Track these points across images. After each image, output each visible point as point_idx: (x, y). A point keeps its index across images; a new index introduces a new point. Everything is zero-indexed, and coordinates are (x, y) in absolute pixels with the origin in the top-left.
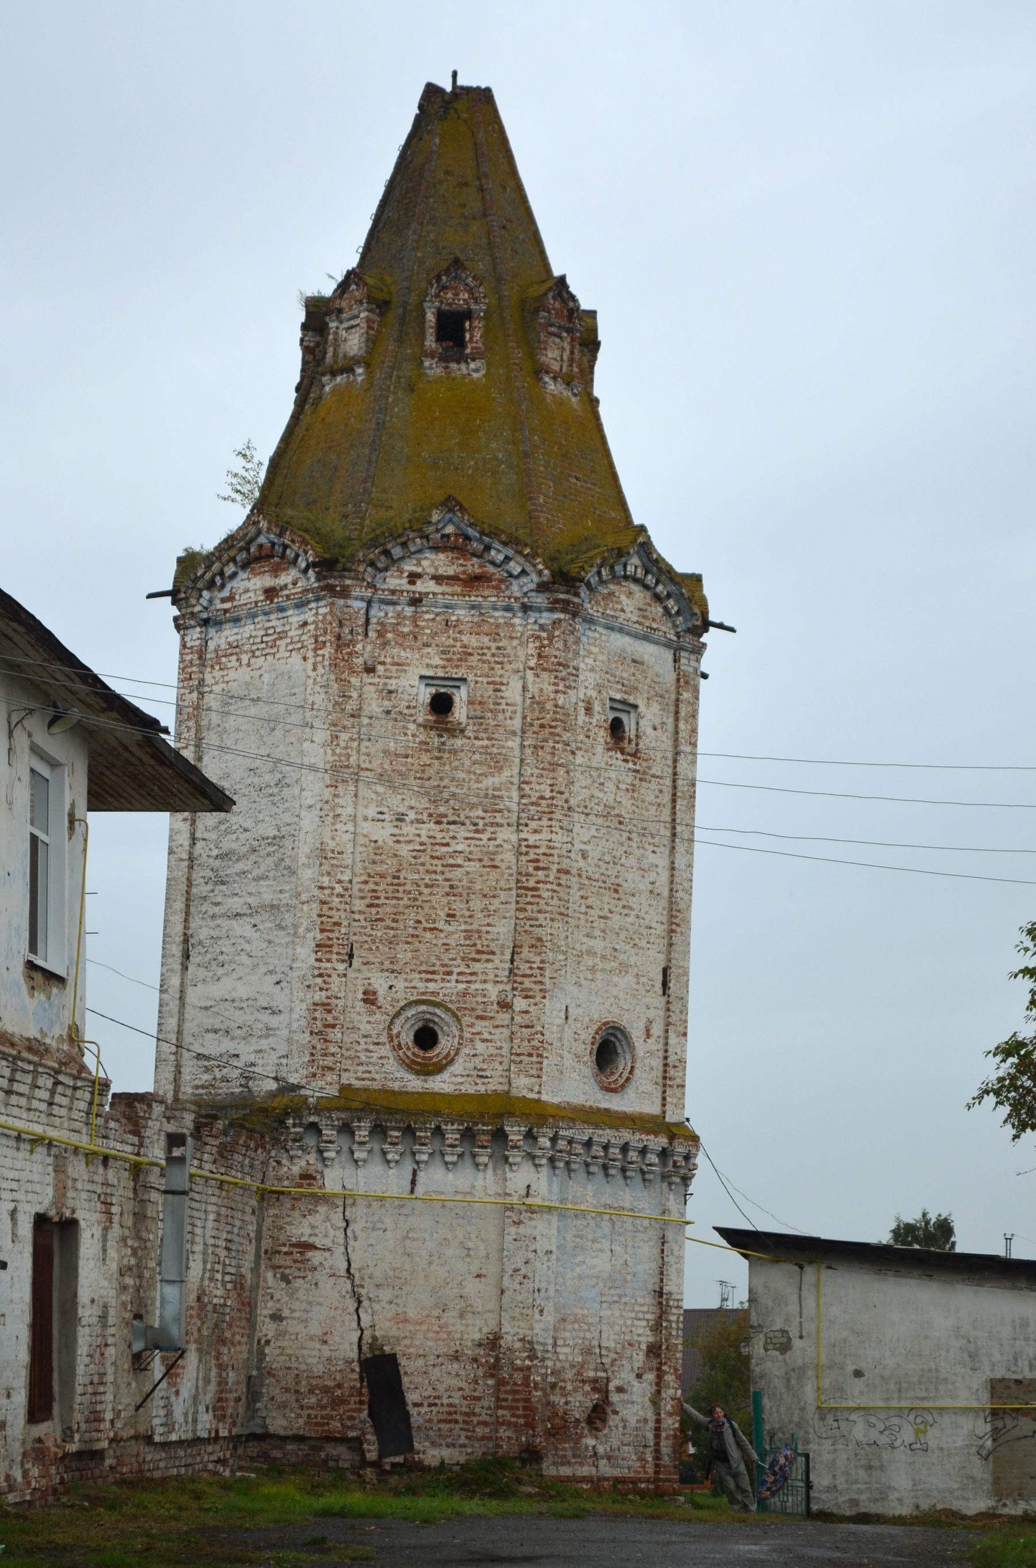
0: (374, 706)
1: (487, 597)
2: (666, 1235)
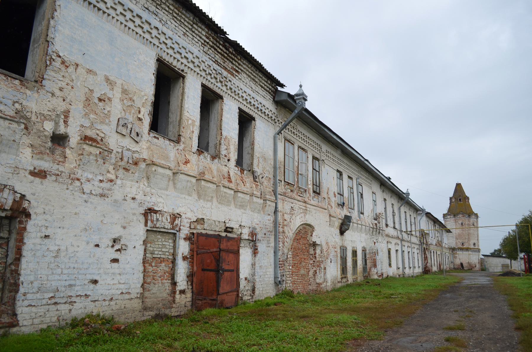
2: (479, 255)
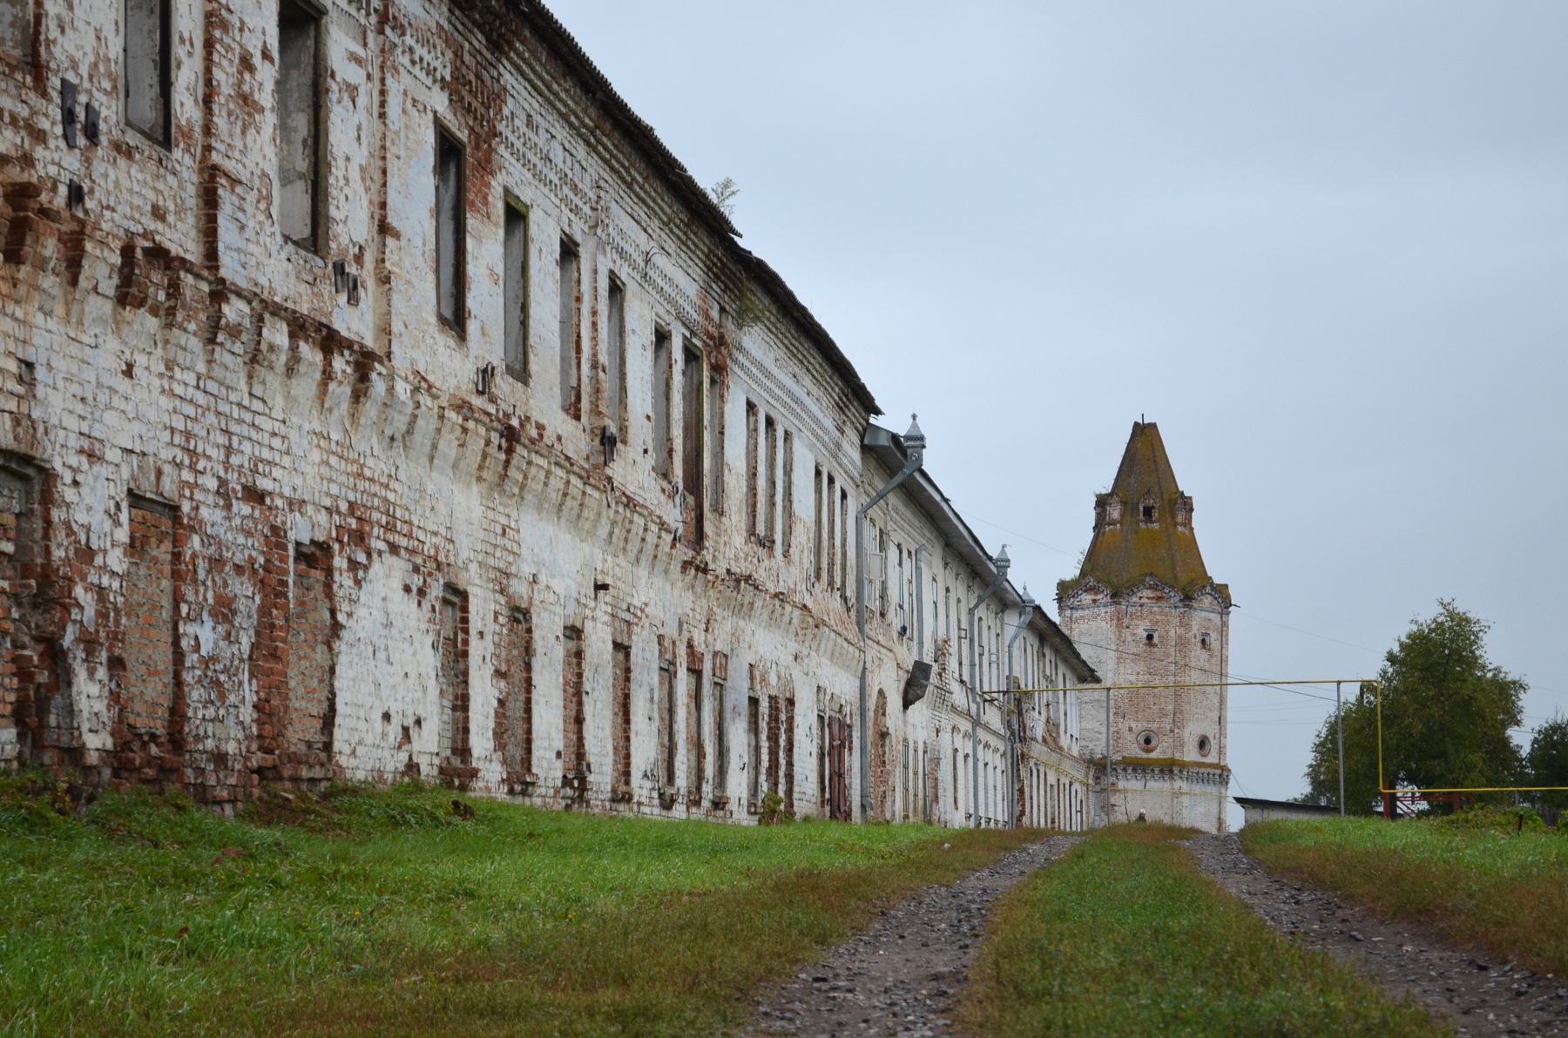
0: (1130, 639)
1: (1164, 604)
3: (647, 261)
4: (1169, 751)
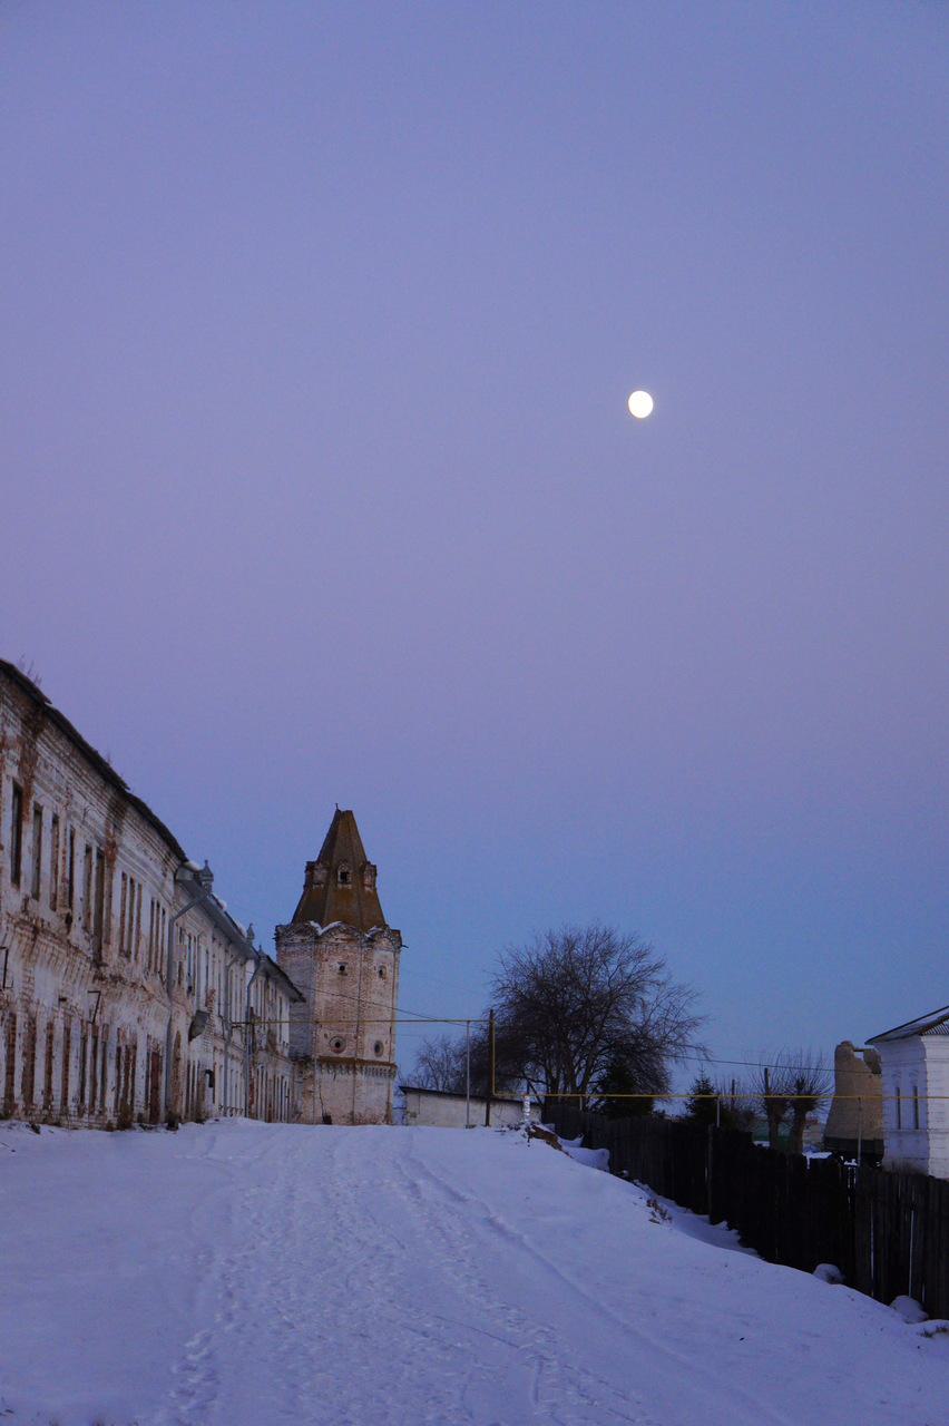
0: (327, 969)
1: (352, 944)
3: (85, 815)
4: (353, 1052)
